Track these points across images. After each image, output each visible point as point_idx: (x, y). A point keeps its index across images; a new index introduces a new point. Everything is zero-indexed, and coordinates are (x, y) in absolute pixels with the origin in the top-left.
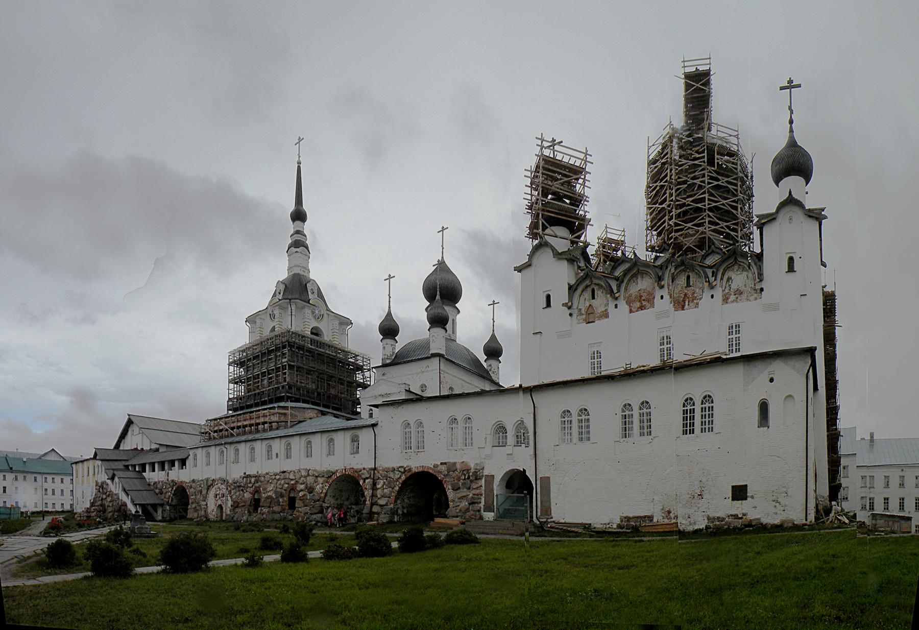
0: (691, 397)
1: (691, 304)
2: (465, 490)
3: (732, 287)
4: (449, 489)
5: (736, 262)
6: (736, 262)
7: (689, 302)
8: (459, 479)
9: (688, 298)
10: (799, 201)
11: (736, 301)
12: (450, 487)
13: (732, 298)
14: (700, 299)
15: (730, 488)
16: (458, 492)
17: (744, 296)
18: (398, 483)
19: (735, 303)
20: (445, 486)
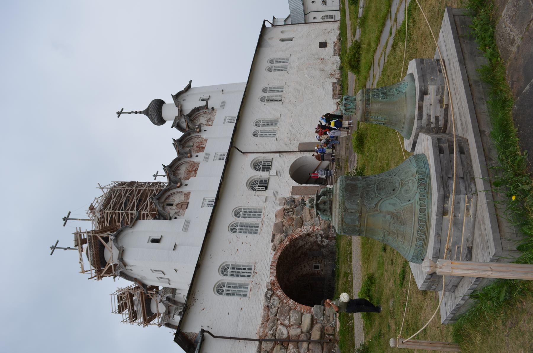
0: (261, 97)
1: (204, 143)
2: (303, 211)
3: (204, 123)
4: (301, 231)
5: (192, 121)
6: (192, 121)
7: (202, 145)
8: (292, 219)
9: (200, 145)
10: (178, 93)
11: (212, 121)
12: (298, 230)
13: (210, 123)
14: (203, 139)
15: (320, 48)
16: (304, 220)
17: (212, 117)
18: (285, 301)
19: (214, 122)
20: (297, 236)
